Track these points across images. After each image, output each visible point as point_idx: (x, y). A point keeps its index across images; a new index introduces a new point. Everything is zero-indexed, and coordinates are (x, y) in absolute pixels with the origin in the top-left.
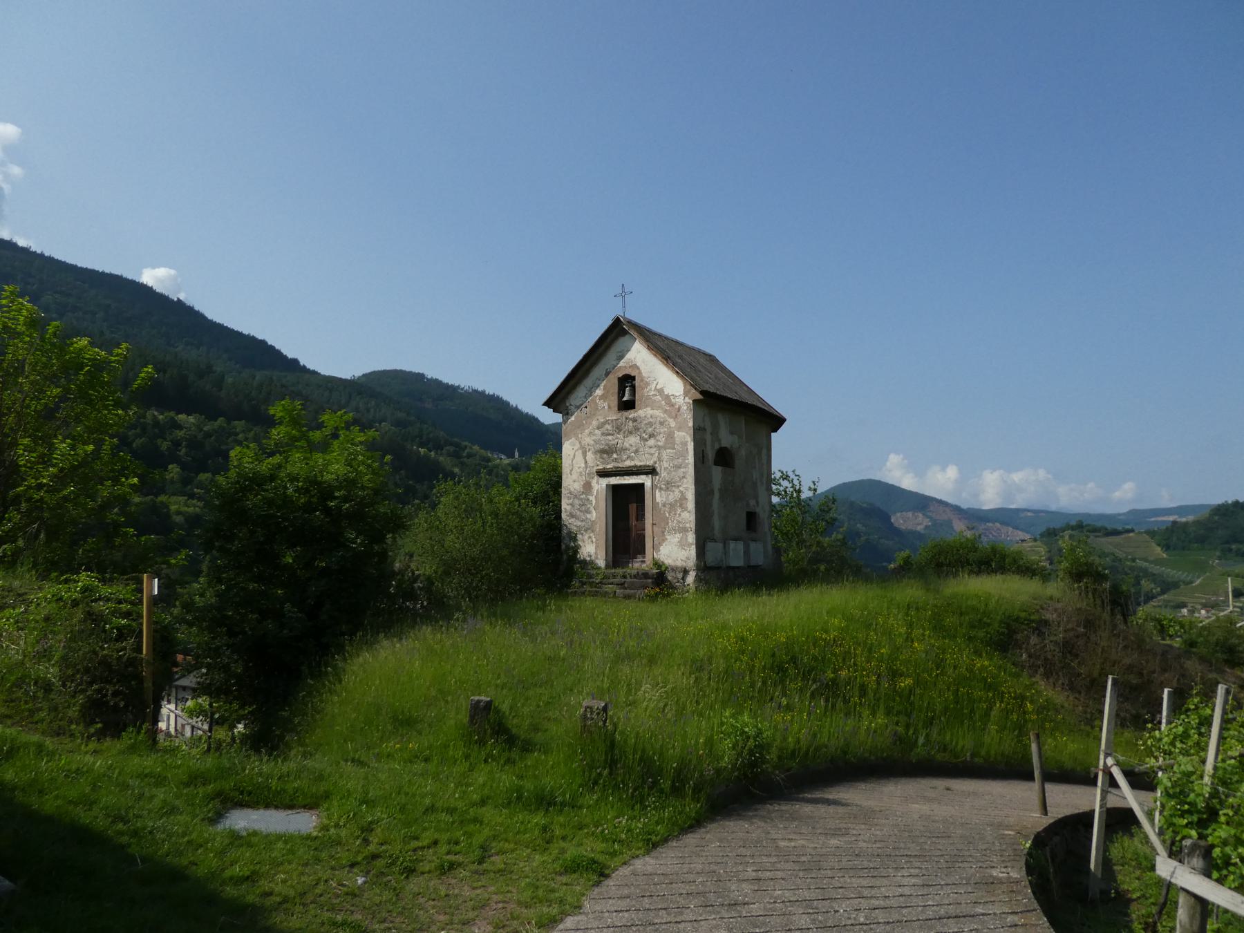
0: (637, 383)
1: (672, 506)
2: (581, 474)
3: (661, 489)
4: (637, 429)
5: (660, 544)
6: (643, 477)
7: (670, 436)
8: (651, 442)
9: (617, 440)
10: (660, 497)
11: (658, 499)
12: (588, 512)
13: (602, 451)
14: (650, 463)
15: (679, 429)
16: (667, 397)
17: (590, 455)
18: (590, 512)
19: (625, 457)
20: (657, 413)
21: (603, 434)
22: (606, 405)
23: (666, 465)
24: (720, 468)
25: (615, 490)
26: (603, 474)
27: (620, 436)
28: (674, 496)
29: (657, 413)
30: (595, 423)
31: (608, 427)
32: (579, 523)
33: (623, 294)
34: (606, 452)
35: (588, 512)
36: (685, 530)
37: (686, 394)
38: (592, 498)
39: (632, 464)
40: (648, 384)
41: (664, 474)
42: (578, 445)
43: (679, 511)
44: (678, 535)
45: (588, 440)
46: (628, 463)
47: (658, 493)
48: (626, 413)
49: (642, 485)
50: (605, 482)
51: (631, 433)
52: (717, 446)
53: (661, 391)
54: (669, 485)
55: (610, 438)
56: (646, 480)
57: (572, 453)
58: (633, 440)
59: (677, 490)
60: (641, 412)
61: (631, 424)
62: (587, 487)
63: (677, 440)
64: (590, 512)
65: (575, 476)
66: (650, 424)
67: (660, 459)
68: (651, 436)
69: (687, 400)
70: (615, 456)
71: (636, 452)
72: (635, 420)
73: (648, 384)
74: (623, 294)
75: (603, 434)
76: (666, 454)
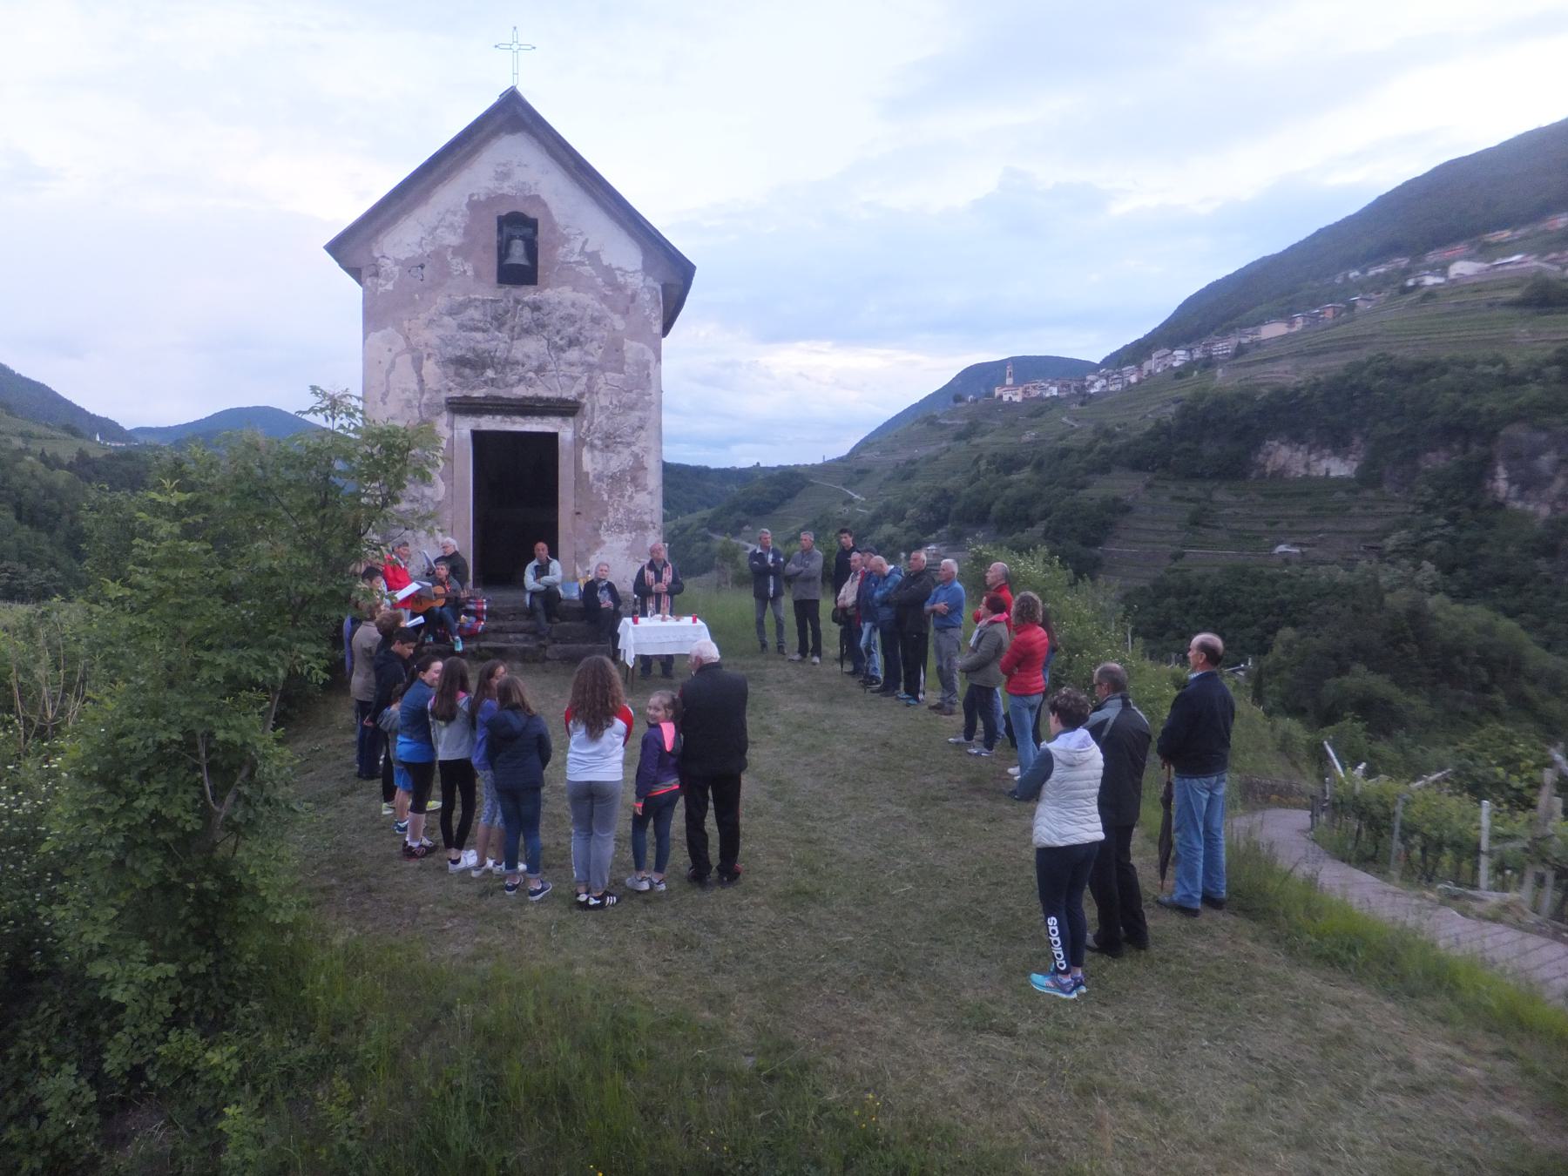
1: (616, 480)
3: (592, 447)
4: (544, 326)
5: (589, 551)
7: (615, 348)
8: (573, 354)
9: (496, 343)
13: (461, 362)
14: (570, 394)
15: (635, 336)
16: (608, 271)
17: (430, 367)
19: (513, 378)
20: (586, 298)
21: (461, 327)
22: (469, 269)
23: (604, 402)
25: (478, 436)
26: (462, 407)
27: (504, 335)
28: (619, 461)
29: (586, 298)
30: (442, 301)
31: (474, 313)
36: (641, 527)
37: (647, 269)
39: (530, 393)
40: (568, 240)
41: (599, 419)
42: (401, 343)
43: (630, 489)
44: (626, 535)
45: (430, 336)
46: (520, 391)
47: (586, 456)
48: (516, 292)
49: (552, 438)
50: (465, 426)
51: (527, 331)
53: (594, 257)
54: (610, 441)
55: (479, 336)
56: (565, 431)
58: (531, 348)
59: (626, 452)
60: (555, 294)
61: (527, 313)
63: (630, 356)
66: (570, 319)
68: (573, 342)
69: (650, 281)
70: (490, 373)
71: (540, 370)
72: (536, 307)
75: (461, 327)
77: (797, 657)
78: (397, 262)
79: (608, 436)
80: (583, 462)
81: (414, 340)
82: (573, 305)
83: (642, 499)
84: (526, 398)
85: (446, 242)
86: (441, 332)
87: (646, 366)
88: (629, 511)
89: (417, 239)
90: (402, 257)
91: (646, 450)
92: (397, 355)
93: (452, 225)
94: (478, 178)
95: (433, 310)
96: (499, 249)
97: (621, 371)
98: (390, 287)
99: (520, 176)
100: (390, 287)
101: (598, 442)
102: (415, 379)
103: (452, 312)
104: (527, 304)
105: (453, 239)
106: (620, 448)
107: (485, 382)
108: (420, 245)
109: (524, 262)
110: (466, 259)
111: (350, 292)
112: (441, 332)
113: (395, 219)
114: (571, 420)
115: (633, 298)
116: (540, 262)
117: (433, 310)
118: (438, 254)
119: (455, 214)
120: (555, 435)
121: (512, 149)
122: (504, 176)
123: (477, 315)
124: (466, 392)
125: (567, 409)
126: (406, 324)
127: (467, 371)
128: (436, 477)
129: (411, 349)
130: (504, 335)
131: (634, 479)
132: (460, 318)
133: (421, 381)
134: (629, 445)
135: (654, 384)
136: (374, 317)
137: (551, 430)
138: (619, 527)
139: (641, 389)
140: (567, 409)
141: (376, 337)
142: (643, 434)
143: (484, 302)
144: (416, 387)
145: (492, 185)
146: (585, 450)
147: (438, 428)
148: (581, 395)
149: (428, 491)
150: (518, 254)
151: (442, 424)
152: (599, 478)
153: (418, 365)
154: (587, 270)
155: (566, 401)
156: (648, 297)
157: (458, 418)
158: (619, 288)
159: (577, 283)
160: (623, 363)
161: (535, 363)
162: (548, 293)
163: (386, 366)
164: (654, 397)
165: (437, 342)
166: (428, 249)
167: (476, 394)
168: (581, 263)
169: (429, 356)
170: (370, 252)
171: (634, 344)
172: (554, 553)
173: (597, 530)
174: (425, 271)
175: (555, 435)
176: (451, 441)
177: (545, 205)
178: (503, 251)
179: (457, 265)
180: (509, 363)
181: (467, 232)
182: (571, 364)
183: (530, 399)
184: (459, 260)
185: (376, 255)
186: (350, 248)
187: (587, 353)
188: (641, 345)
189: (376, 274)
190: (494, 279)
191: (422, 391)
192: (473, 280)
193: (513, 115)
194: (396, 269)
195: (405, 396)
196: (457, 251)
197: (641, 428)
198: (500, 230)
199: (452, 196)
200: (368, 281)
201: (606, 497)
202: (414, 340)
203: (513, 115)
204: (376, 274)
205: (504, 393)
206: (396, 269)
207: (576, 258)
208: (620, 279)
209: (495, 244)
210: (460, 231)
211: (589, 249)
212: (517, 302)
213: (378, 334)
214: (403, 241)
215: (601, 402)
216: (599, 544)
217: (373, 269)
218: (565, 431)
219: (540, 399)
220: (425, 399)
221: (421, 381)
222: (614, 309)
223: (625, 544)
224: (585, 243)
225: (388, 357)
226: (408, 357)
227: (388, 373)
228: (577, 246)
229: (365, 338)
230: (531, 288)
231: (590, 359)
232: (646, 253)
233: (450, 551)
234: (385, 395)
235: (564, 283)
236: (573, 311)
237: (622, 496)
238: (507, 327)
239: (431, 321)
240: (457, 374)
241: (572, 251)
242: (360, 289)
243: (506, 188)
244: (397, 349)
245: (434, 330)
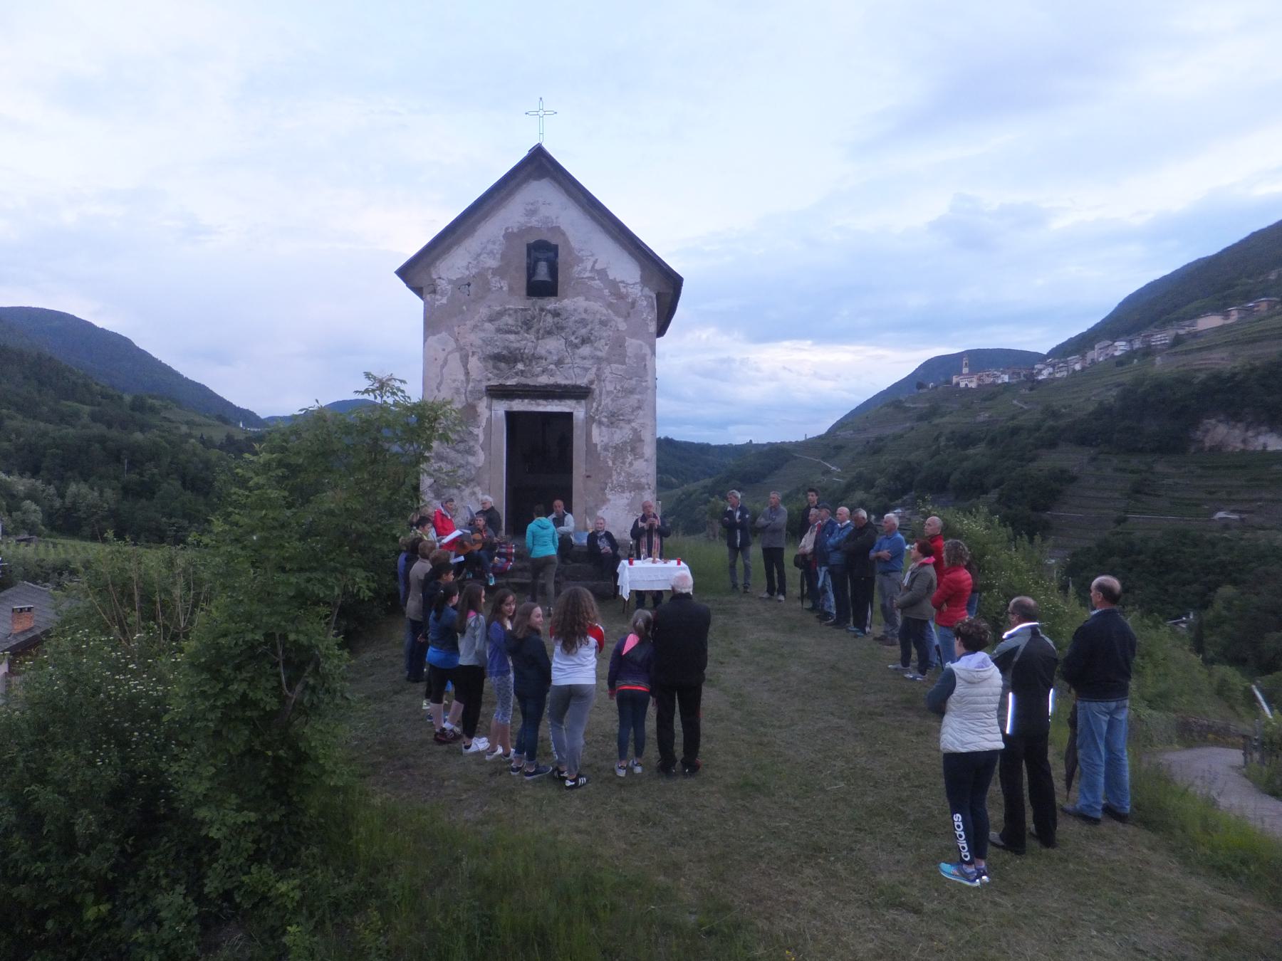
0: (562, 253)
1: (619, 450)
2: (457, 391)
3: (600, 423)
4: (562, 328)
5: (597, 507)
7: (618, 344)
8: (585, 350)
9: (524, 342)
10: (599, 436)
12: (470, 452)
13: (497, 358)
14: (582, 382)
15: (634, 335)
16: (614, 284)
17: (474, 362)
18: (473, 454)
21: (498, 330)
23: (610, 387)
25: (510, 415)
27: (531, 337)
28: (622, 434)
29: (595, 306)
30: (484, 311)
31: (509, 320)
35: (470, 452)
36: (639, 487)
37: (645, 281)
38: (479, 432)
39: (551, 381)
40: (581, 260)
41: (606, 401)
42: (452, 345)
43: (630, 458)
44: (627, 494)
45: (474, 338)
46: (544, 380)
47: (595, 431)
49: (569, 416)
50: (501, 408)
51: (550, 333)
53: (602, 274)
54: (614, 419)
55: (512, 337)
56: (579, 411)
58: (553, 345)
59: (628, 427)
60: (571, 303)
61: (549, 319)
62: (470, 411)
63: (630, 352)
64: (473, 454)
66: (583, 323)
67: (598, 376)
68: (585, 341)
69: (647, 291)
70: (520, 366)
71: (559, 363)
72: (556, 314)
73: (581, 260)
75: (498, 330)
77: (766, 595)
78: (450, 282)
79: (613, 415)
80: (593, 435)
81: (462, 342)
82: (586, 311)
83: (640, 465)
84: (547, 386)
85: (487, 265)
86: (482, 335)
87: (643, 358)
88: (629, 475)
89: (465, 264)
90: (454, 278)
91: (643, 426)
92: (449, 353)
93: (491, 252)
94: (512, 215)
95: (477, 318)
96: (528, 268)
97: (623, 363)
98: (444, 301)
99: (544, 211)
100: (444, 301)
101: (605, 420)
102: (462, 371)
103: (491, 320)
104: (549, 311)
105: (493, 263)
106: (622, 424)
107: (516, 374)
108: (467, 268)
109: (547, 279)
110: (502, 278)
111: (416, 305)
112: (482, 335)
114: (583, 402)
115: (633, 304)
116: (560, 278)
117: (477, 318)
118: (481, 275)
119: (494, 243)
120: (571, 414)
122: (532, 213)
123: (510, 321)
124: (501, 381)
125: (580, 393)
126: (456, 329)
127: (503, 365)
128: (477, 448)
129: (460, 348)
130: (531, 337)
131: (633, 450)
132: (497, 323)
133: (467, 373)
134: (629, 421)
135: (650, 372)
136: (431, 324)
137: (567, 410)
139: (640, 378)
140: (580, 393)
141: (432, 339)
142: (641, 413)
143: (516, 311)
144: (462, 377)
145: (523, 220)
146: (594, 426)
147: (479, 410)
148: (592, 382)
149: (471, 459)
150: (542, 273)
151: (482, 406)
152: (606, 448)
153: (465, 361)
154: (597, 283)
155: (580, 387)
156: (645, 303)
157: (495, 402)
158: (621, 297)
159: (588, 293)
160: (625, 356)
161: (555, 358)
162: (566, 302)
163: (440, 362)
164: (650, 384)
165: (480, 342)
166: (474, 271)
167: (509, 383)
168: (593, 279)
169: (473, 353)
170: (430, 275)
171: (633, 341)
172: (569, 508)
173: (603, 489)
174: (471, 288)
175: (571, 414)
176: (489, 420)
177: (563, 234)
178: (531, 271)
179: (495, 282)
180: (535, 358)
181: (503, 256)
182: (584, 358)
183: (552, 385)
184: (497, 278)
185: (435, 277)
186: (415, 272)
187: (596, 349)
188: (640, 342)
189: (434, 292)
190: (524, 292)
191: (468, 381)
192: (508, 295)
193: (539, 164)
194: (449, 287)
195: (454, 385)
196: (495, 272)
197: (639, 408)
198: (529, 255)
199: (492, 229)
200: (428, 297)
201: (610, 463)
202: (462, 342)
203: (539, 164)
204: (434, 292)
205: (530, 382)
206: (449, 287)
207: (587, 274)
208: (623, 290)
209: (525, 265)
210: (498, 256)
211: (598, 267)
212: (542, 310)
213: (435, 338)
214: (455, 266)
215: (607, 390)
216: (605, 501)
217: (431, 288)
218: (579, 411)
219: (559, 386)
220: (469, 388)
221: (467, 373)
222: (617, 313)
223: (626, 501)
224: (595, 262)
225: (442, 355)
226: (457, 355)
227: (443, 367)
228: (589, 268)
229: (425, 341)
230: (553, 299)
231: (599, 354)
232: (643, 268)
233: (488, 506)
234: (440, 384)
235: (578, 295)
236: (584, 316)
237: (624, 463)
238: (533, 330)
239: (475, 327)
240: (495, 367)
241: (585, 269)
242: (421, 302)
243: (534, 222)
244: (449, 349)
245: (478, 334)
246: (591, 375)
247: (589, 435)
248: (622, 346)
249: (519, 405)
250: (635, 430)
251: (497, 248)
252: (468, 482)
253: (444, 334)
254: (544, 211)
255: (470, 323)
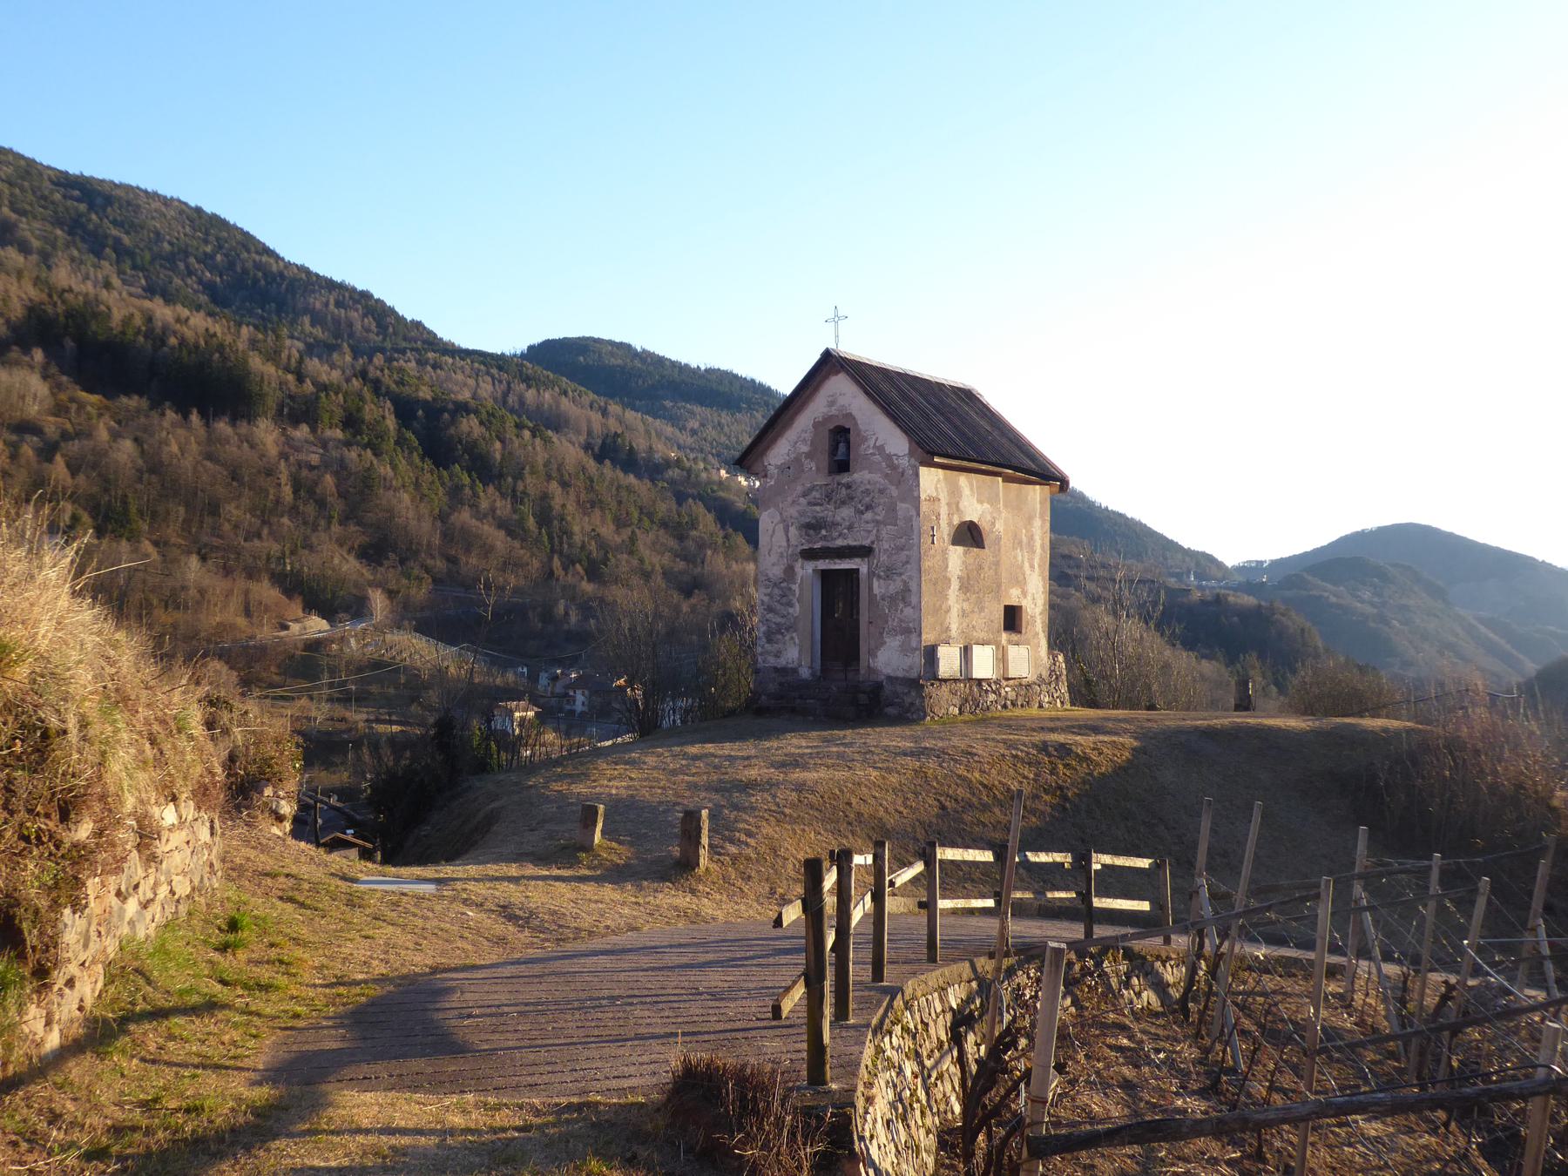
1: (893, 599)
3: (879, 577)
5: (877, 648)
6: (858, 560)
7: (892, 509)
8: (868, 515)
9: (825, 512)
10: (878, 587)
11: (876, 590)
14: (866, 543)
15: (903, 500)
16: (889, 457)
17: (793, 531)
19: (835, 534)
20: (877, 477)
21: (810, 504)
22: (813, 465)
24: (960, 549)
25: (825, 575)
26: (809, 555)
27: (831, 507)
28: (895, 586)
29: (877, 477)
30: (799, 489)
31: (815, 494)
32: (779, 620)
33: (837, 319)
34: (813, 527)
37: (911, 453)
38: (795, 587)
40: (865, 439)
41: (883, 558)
45: (793, 511)
46: (840, 542)
47: (875, 583)
48: (838, 478)
51: (843, 503)
52: (956, 521)
53: (881, 449)
54: (890, 572)
55: (818, 508)
57: (771, 528)
58: (846, 513)
60: (860, 476)
62: (790, 571)
63: (900, 514)
65: (774, 558)
66: (867, 492)
68: (868, 507)
70: (824, 532)
71: (850, 528)
72: (848, 486)
74: (837, 319)
75: (810, 504)
76: (887, 531)
78: (777, 467)
91: (910, 578)
94: (817, 408)
99: (841, 401)
103: (804, 495)
105: (805, 449)
113: (774, 441)
118: (797, 460)
121: (840, 387)
122: (832, 404)
125: (865, 552)
138: (894, 632)
140: (865, 552)
158: (894, 467)
178: (834, 450)
180: (835, 524)
192: (815, 474)
193: (829, 364)
196: (809, 455)
205: (830, 544)
218: (864, 569)
219: (849, 548)
222: (891, 483)
228: (872, 443)
243: (833, 411)
246: (872, 538)
247: (870, 588)
248: (894, 510)
249: (823, 565)
250: (905, 582)
251: (808, 436)
252: (787, 629)
253: (772, 510)
254: (841, 401)
255: (790, 499)
